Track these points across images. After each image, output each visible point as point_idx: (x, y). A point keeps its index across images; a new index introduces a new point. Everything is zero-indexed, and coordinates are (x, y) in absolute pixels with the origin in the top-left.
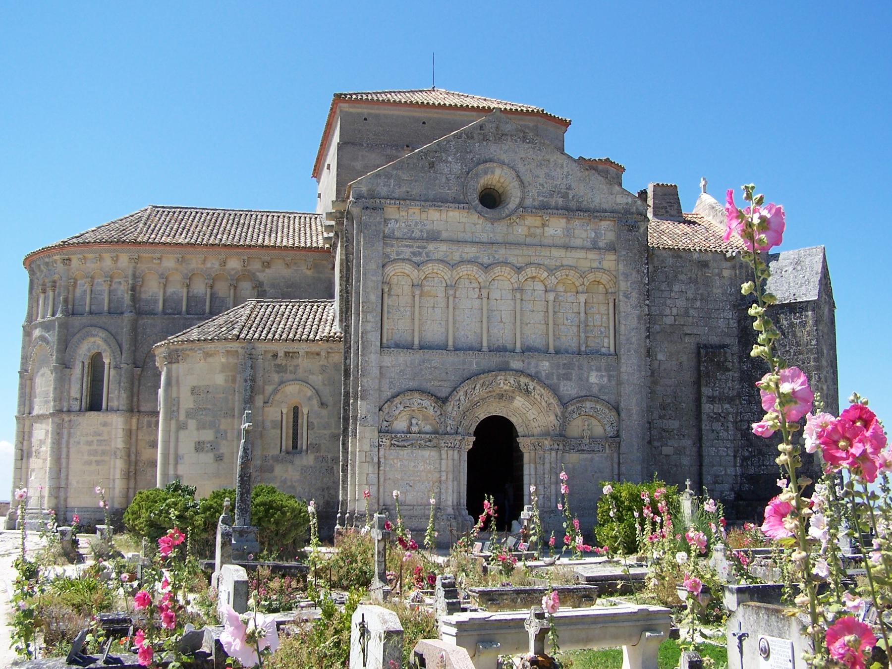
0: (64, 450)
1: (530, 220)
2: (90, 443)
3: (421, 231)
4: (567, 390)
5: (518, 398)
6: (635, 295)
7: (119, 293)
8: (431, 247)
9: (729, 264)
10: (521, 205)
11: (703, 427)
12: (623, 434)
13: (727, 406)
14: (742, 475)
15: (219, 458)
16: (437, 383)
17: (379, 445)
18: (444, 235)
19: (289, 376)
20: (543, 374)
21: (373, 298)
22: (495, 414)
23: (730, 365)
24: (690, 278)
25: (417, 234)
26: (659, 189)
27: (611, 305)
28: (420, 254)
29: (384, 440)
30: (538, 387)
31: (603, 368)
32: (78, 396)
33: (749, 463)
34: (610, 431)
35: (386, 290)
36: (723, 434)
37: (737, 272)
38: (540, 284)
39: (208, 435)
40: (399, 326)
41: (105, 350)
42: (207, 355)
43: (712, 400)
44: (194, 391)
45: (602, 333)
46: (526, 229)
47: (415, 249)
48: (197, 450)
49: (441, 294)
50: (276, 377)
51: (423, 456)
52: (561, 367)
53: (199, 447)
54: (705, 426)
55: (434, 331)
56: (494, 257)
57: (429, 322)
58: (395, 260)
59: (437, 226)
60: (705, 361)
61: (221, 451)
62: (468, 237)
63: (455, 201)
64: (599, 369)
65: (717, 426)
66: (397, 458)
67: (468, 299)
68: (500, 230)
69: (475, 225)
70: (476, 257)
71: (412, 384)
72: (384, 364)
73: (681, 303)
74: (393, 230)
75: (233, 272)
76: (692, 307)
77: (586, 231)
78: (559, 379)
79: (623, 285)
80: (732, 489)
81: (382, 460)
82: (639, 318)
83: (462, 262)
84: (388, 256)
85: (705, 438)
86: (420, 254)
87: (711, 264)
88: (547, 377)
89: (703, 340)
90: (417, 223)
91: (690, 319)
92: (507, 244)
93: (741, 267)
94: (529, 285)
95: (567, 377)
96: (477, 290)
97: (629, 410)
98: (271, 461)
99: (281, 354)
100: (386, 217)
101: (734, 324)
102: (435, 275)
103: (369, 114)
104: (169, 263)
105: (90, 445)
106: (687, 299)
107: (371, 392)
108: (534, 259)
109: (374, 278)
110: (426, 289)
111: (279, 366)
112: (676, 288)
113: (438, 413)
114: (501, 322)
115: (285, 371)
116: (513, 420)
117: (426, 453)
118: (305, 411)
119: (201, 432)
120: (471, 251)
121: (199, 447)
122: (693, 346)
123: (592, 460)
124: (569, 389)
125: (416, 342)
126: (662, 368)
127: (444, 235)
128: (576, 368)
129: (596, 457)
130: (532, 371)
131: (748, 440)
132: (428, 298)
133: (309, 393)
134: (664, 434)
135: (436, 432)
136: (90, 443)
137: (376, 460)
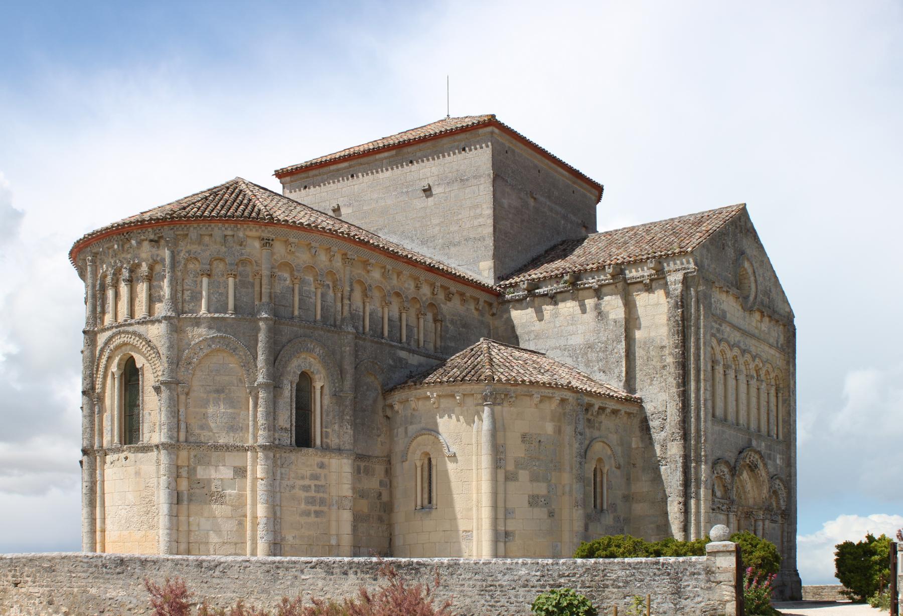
2: (306, 488)
15: (551, 514)
32: (288, 426)
39: (541, 489)
41: (318, 372)
44: (524, 437)
53: (534, 501)
75: (424, 299)
99: (596, 407)
105: (307, 491)
111: (589, 420)
118: (605, 471)
119: (535, 484)
121: (534, 501)
133: (609, 452)
136: (306, 488)
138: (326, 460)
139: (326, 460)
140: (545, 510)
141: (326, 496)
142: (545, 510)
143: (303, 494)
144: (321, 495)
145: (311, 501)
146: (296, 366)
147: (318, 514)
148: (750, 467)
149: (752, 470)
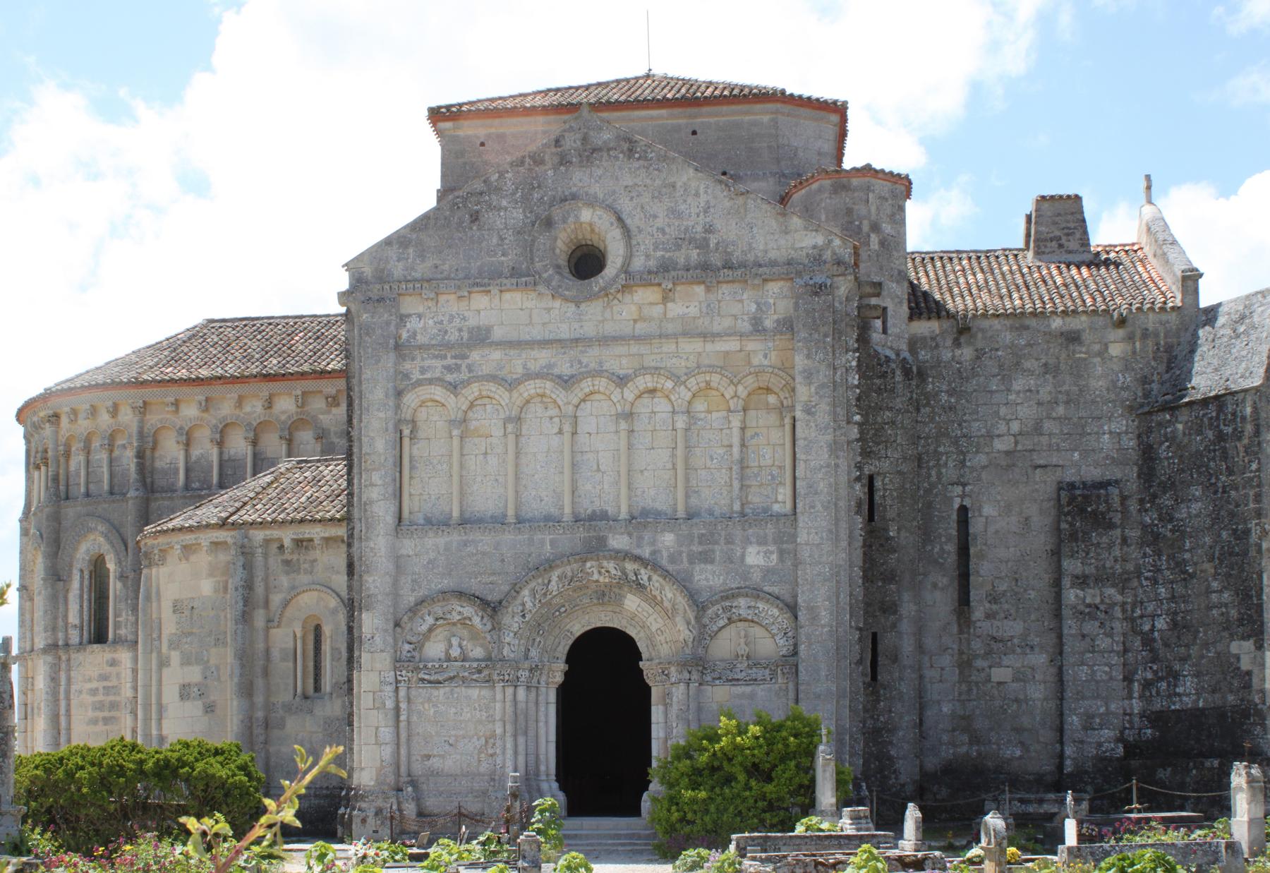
0: (63, 704)
1: (646, 295)
3: (460, 330)
4: (707, 580)
5: (629, 596)
6: (824, 407)
7: (125, 461)
8: (475, 356)
9: (1121, 333)
10: (625, 269)
11: (1065, 631)
12: (802, 648)
13: (1112, 591)
14: (1142, 715)
15: (209, 709)
17: (397, 682)
18: (498, 334)
19: (303, 579)
20: (665, 554)
21: (380, 445)
22: (599, 625)
23: (1117, 519)
24: (1045, 365)
25: (453, 336)
26: (1046, 205)
27: (788, 428)
28: (457, 368)
29: (404, 673)
30: (655, 577)
31: (770, 538)
32: (77, 622)
33: (1154, 693)
34: (783, 645)
35: (406, 432)
36: (1103, 643)
37: (1138, 345)
38: (664, 401)
40: (431, 490)
42: (188, 550)
43: (1082, 581)
44: (177, 608)
45: (773, 478)
46: (634, 308)
47: (449, 361)
48: (182, 697)
49: (497, 432)
50: (284, 581)
51: (468, 698)
52: (696, 540)
54: (1070, 626)
55: (486, 498)
56: (580, 362)
57: (479, 479)
58: (418, 380)
59: (484, 320)
60: (1068, 513)
61: (212, 698)
62: (536, 333)
63: (515, 273)
64: (762, 542)
65: (1091, 627)
66: (429, 700)
67: (542, 439)
68: (594, 316)
69: (549, 310)
70: (550, 366)
71: (446, 583)
72: (404, 552)
73: (1027, 411)
74: (415, 334)
76: (1049, 418)
77: (741, 301)
78: (691, 562)
79: (804, 393)
80: (1121, 739)
81: (403, 706)
82: (834, 448)
83: (529, 376)
84: (406, 376)
85: (1067, 649)
86: (457, 368)
87: (1086, 337)
88: (672, 559)
89: (1070, 476)
90: (452, 317)
91: (1044, 440)
92: (605, 341)
93: (1145, 335)
94: (644, 406)
95: (706, 558)
96: (556, 420)
97: (811, 609)
98: (281, 712)
100: (403, 311)
101: (1130, 443)
102: (486, 401)
103: (489, 136)
104: (190, 411)
105: (94, 695)
106: (1039, 404)
107: (380, 598)
108: (650, 361)
109: (382, 415)
110: (473, 425)
111: (287, 563)
112: (1018, 384)
113: (489, 626)
114: (598, 470)
115: (298, 571)
116: (632, 632)
117: (474, 693)
120: (542, 357)
122: (1051, 489)
123: (752, 696)
124: (708, 577)
125: (456, 514)
126: (991, 529)
127: (498, 334)
128: (722, 541)
129: (760, 691)
130: (646, 552)
131: (1151, 651)
132: (476, 440)
134: (995, 646)
135: (489, 659)
136: (94, 692)
137: (390, 704)
138: (116, 656)
139: (116, 656)
140: (199, 703)
141: (118, 698)
142: (199, 703)
143: (89, 699)
144: (112, 698)
145: (99, 707)
146: (83, 552)
147: (106, 721)
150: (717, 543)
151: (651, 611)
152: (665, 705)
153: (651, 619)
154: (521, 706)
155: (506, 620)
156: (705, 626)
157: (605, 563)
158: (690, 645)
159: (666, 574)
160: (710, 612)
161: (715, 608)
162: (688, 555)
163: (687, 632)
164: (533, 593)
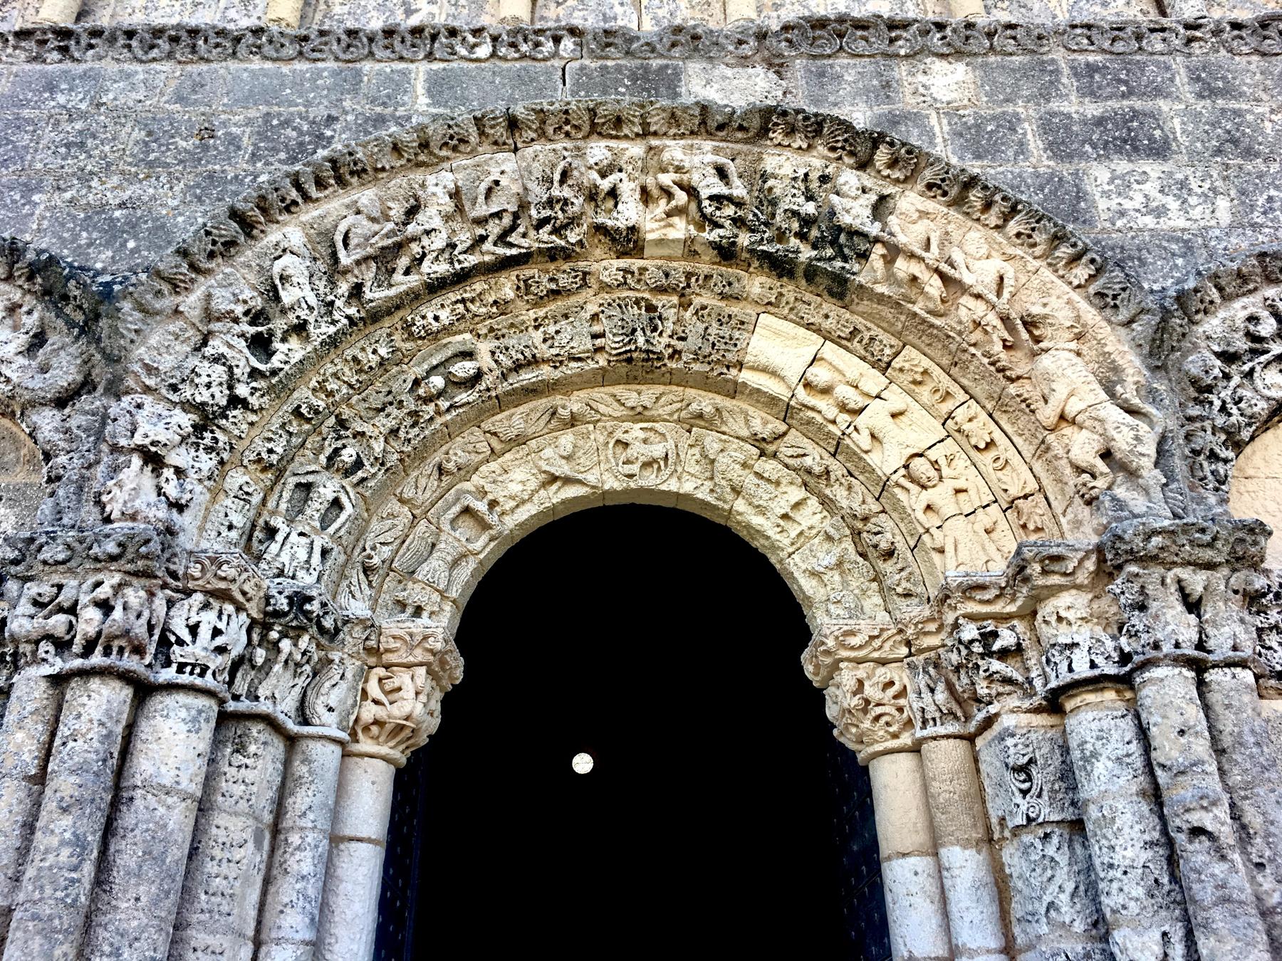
16: (108, 191)
20: (940, 126)
30: (910, 201)
148: (780, 266)
149: (840, 288)
150: (1159, 92)
151: (873, 380)
152: (989, 842)
153: (876, 416)
154: (159, 817)
155: (158, 347)
156: (1202, 390)
157: (674, 150)
158: (1152, 476)
159: (959, 190)
160: (1212, 325)
161: (1239, 309)
162: (1046, 126)
163: (1114, 414)
164: (327, 250)
